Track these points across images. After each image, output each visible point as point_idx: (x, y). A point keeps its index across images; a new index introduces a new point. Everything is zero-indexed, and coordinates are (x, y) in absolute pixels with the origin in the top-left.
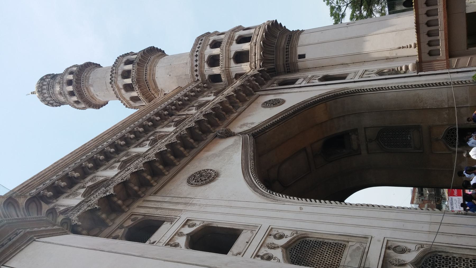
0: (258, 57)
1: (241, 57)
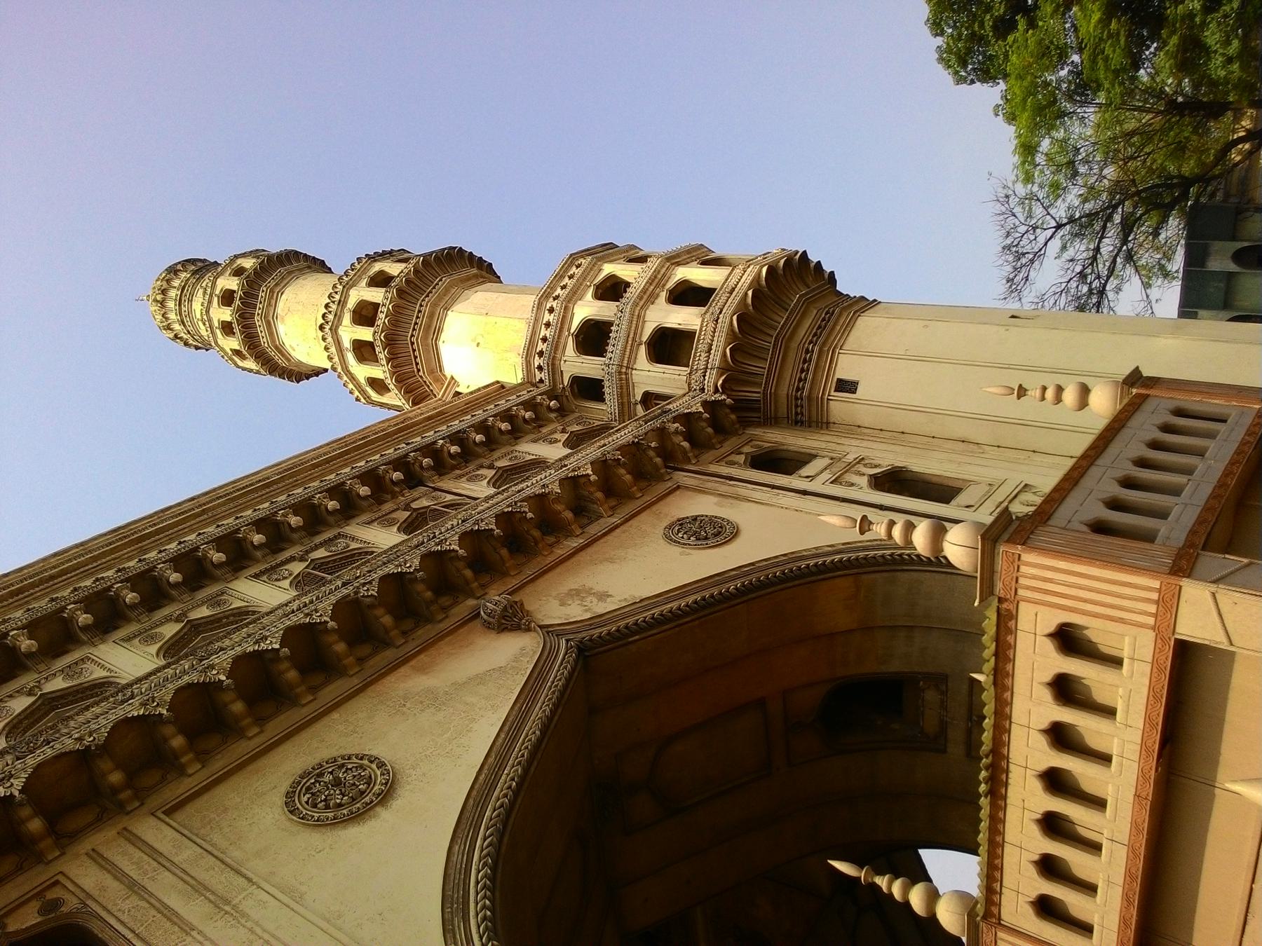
0: (716, 359)
1: (669, 346)
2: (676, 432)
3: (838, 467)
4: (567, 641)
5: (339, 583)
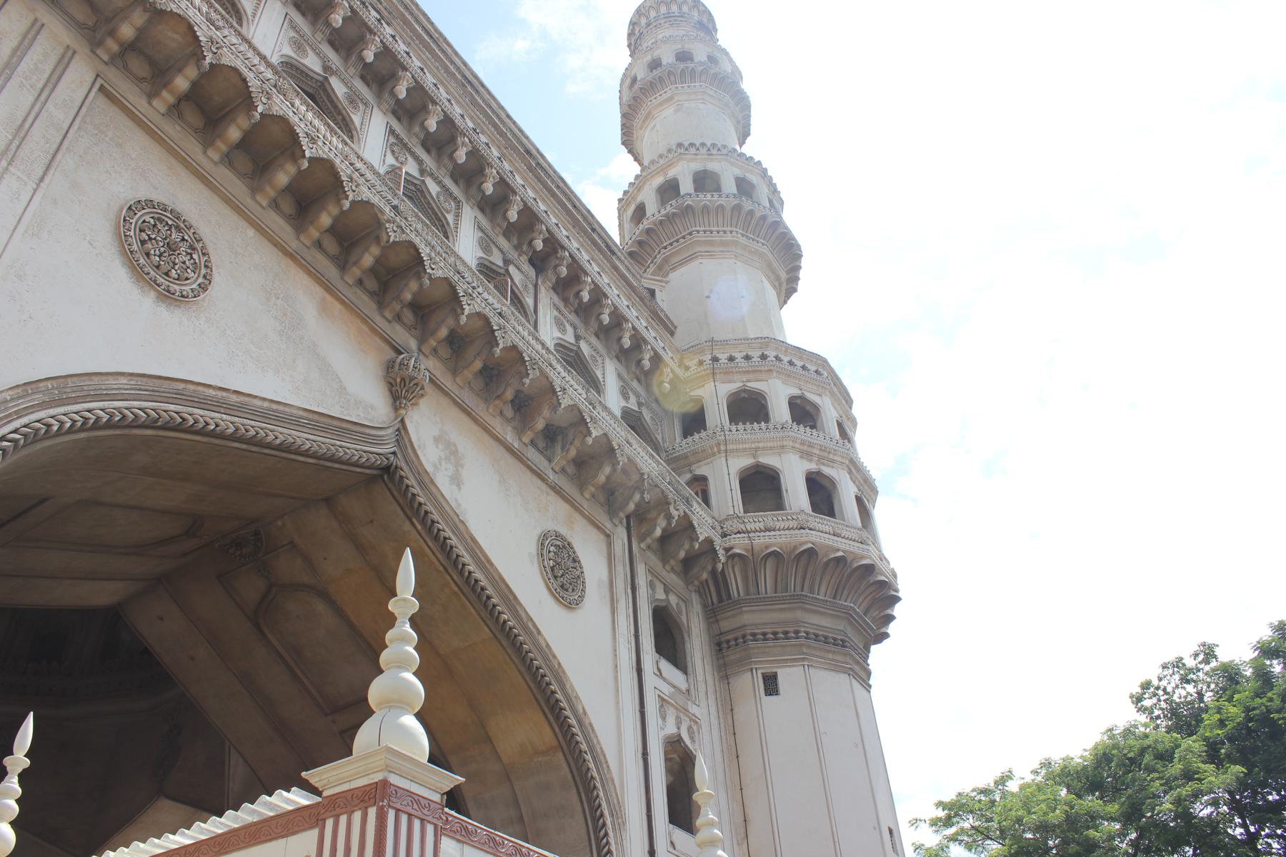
0: (760, 540)
2: (669, 517)
4: (394, 453)
5: (395, 202)
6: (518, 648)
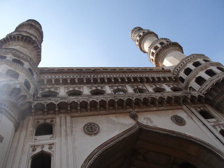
0: (207, 88)
2: (189, 98)
3: (217, 123)
6: (179, 138)
